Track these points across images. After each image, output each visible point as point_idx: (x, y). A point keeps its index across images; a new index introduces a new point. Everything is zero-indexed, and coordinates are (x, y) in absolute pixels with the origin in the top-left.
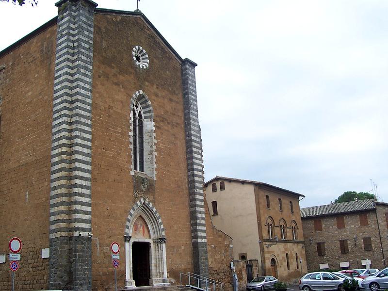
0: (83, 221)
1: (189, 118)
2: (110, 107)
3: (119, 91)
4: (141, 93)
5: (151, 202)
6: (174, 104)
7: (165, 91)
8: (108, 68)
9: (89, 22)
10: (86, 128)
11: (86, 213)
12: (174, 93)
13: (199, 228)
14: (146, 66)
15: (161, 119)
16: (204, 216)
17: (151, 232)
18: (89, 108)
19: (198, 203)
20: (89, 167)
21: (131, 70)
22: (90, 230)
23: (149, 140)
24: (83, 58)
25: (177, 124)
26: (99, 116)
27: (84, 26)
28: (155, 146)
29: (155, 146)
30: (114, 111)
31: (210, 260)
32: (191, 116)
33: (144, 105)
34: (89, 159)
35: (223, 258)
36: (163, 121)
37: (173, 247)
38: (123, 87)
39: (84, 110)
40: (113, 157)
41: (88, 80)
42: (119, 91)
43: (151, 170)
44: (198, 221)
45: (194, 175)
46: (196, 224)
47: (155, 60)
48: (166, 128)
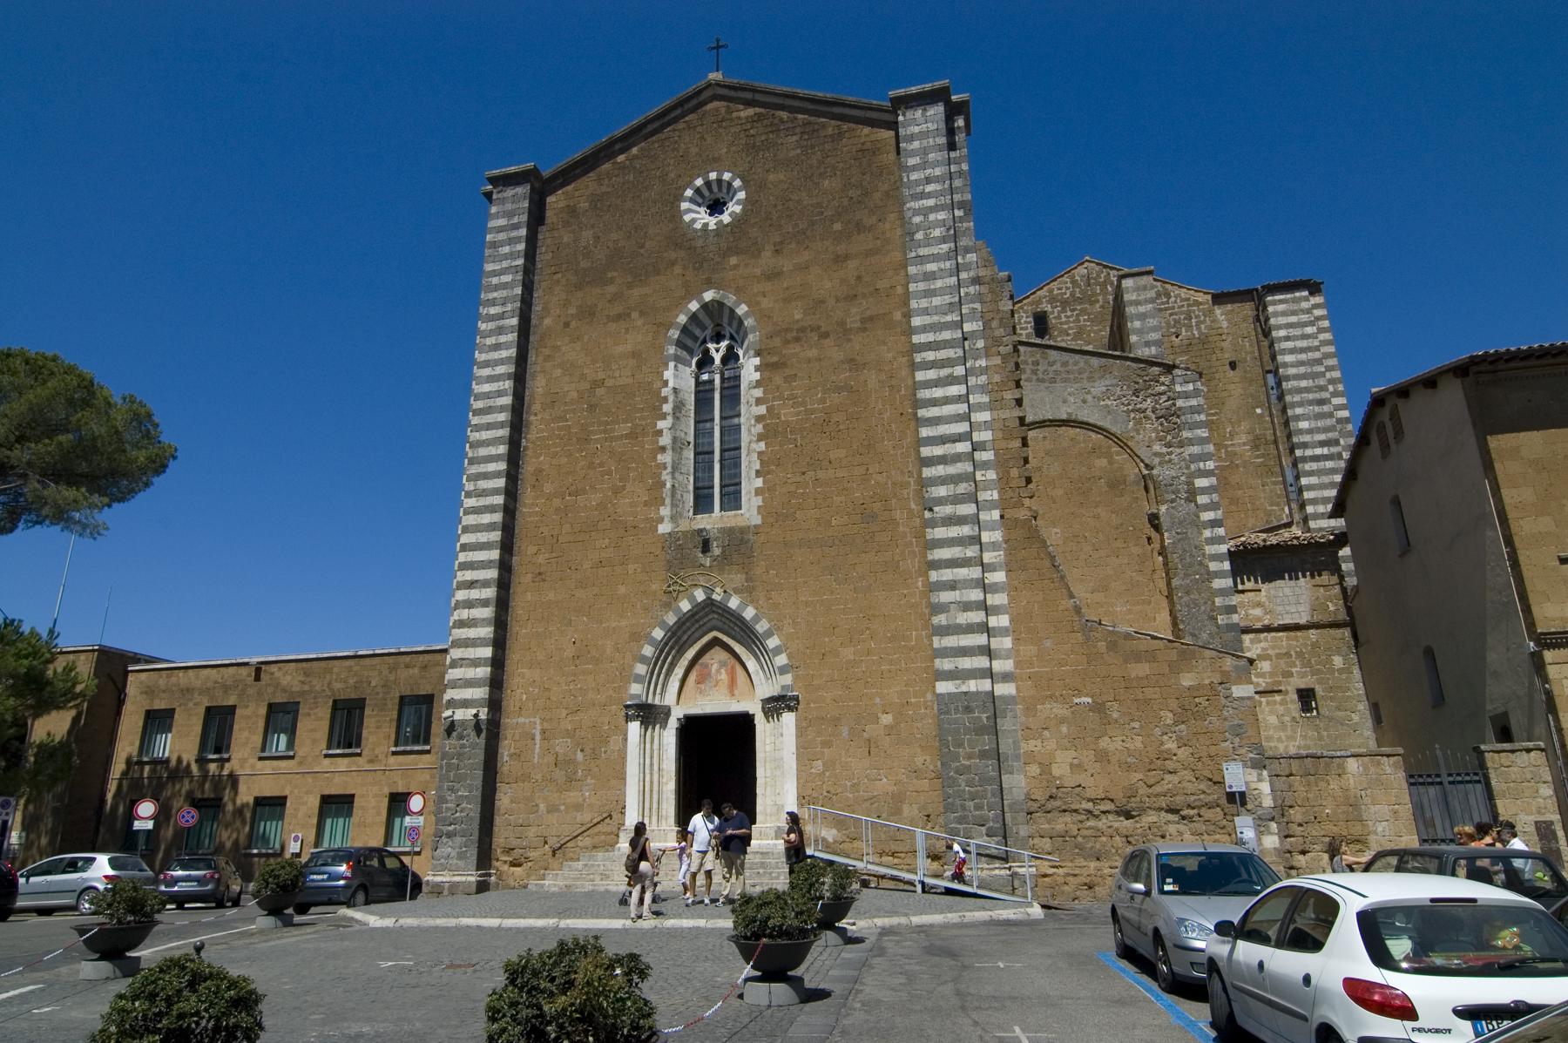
2: (598, 384)
5: (736, 591)
6: (852, 264)
9: (516, 220)
11: (475, 663)
21: (673, 255)
25: (871, 319)
36: (797, 340)
38: (642, 314)
40: (601, 506)
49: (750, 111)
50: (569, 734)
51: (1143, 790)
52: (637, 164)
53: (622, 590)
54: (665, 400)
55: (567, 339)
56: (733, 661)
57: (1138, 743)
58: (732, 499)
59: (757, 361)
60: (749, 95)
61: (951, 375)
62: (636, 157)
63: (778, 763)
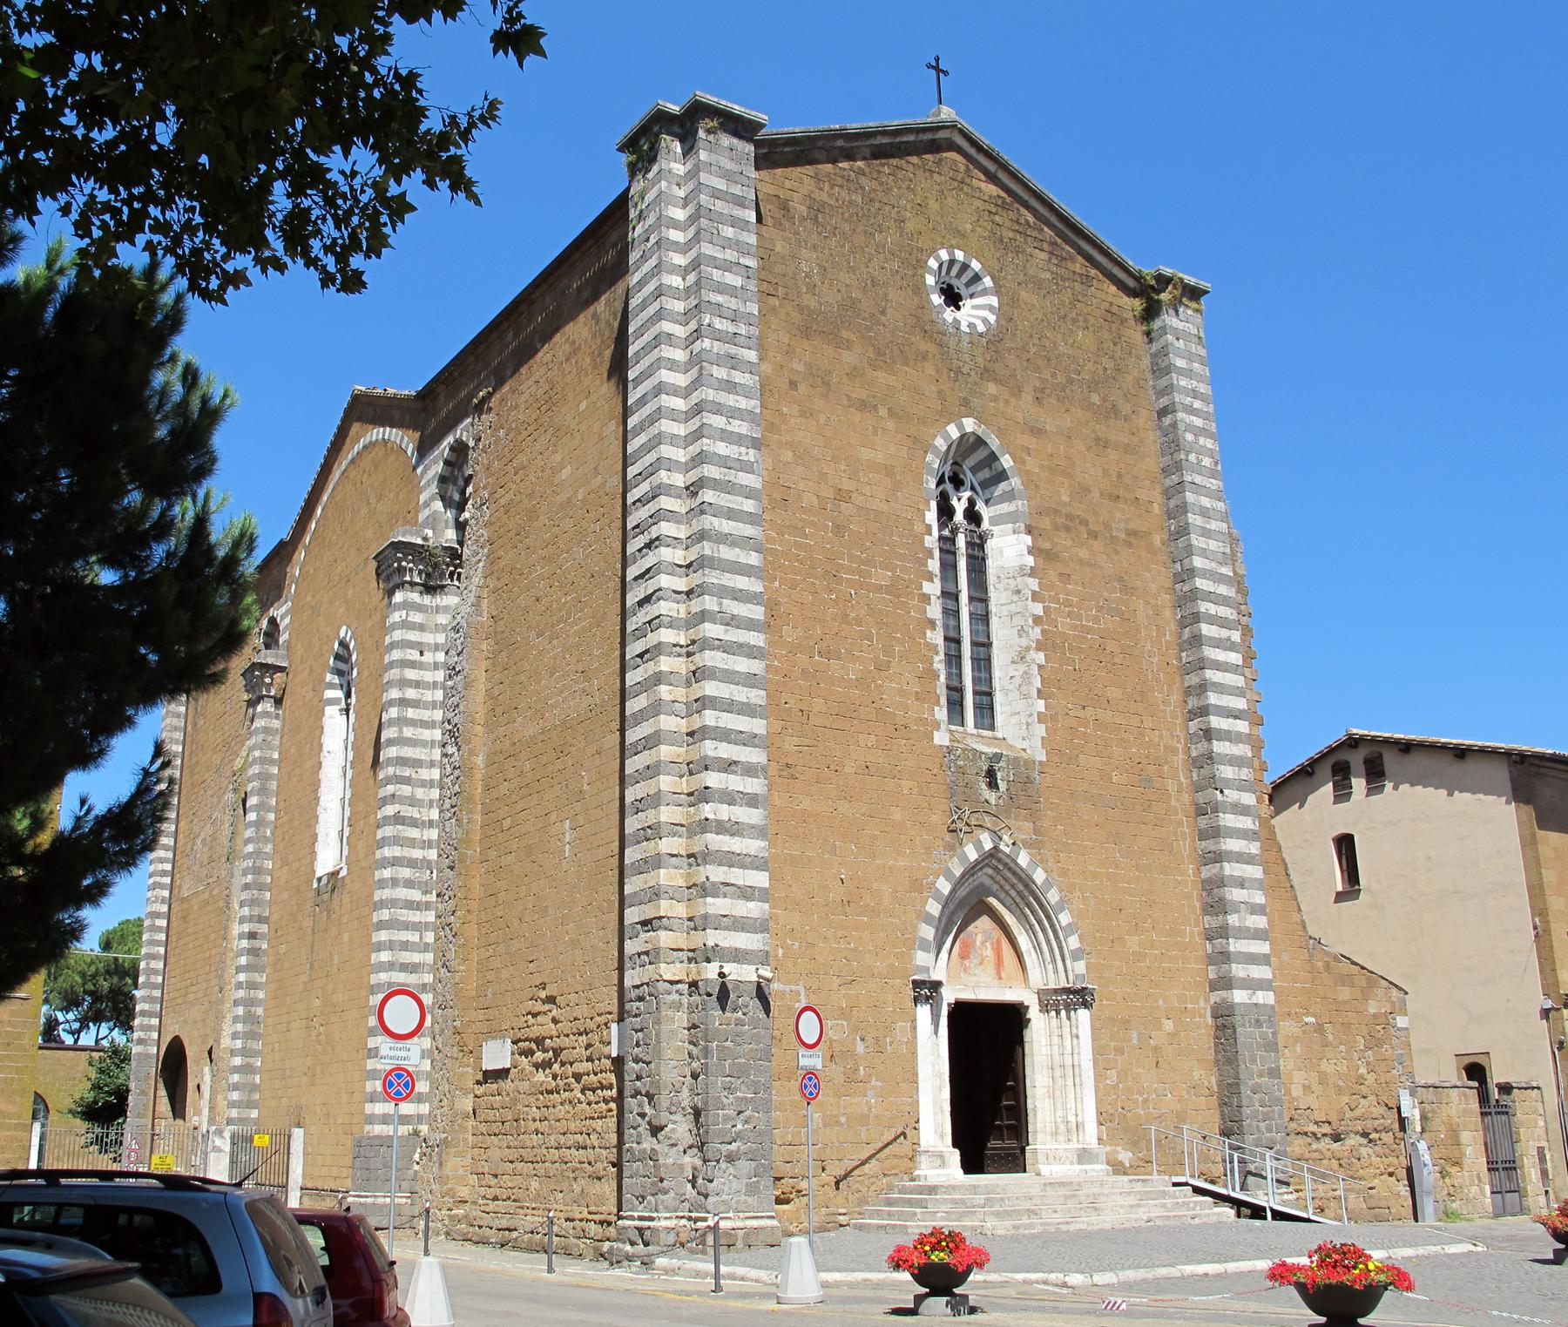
0: (740, 925)
1: (1183, 508)
2: (842, 496)
3: (875, 432)
4: (969, 430)
5: (1028, 845)
6: (1113, 455)
7: (1073, 410)
8: (829, 350)
9: (737, 190)
10: (742, 582)
11: (747, 893)
12: (1115, 411)
13: (1235, 946)
14: (985, 321)
15: (1061, 520)
16: (1259, 898)
17: (1031, 959)
18: (749, 506)
19: (1232, 845)
20: (758, 726)
21: (924, 346)
22: (764, 958)
23: (1013, 608)
24: (720, 324)
25: (1133, 533)
26: (798, 530)
27: (720, 206)
28: (1038, 630)
29: (1038, 630)
30: (860, 508)
31: (1299, 1078)
32: (1190, 497)
33: (985, 474)
34: (756, 696)
35: (1362, 1070)
36: (1068, 529)
37: (1126, 1023)
39: (731, 514)
40: (861, 682)
41: (743, 403)
42: (875, 432)
43: (1019, 725)
44: (1233, 919)
45: (1208, 734)
46: (1223, 932)
47: (1023, 294)
48: (1083, 553)
49: (992, 189)
50: (843, 1014)
51: (1348, 1114)
52: (863, 181)
53: (897, 815)
54: (930, 554)
55: (795, 410)
56: (997, 933)
57: (1343, 1067)
58: (986, 711)
59: (1028, 540)
60: (992, 167)
61: (1229, 639)
62: (861, 172)
63: (1064, 1071)
